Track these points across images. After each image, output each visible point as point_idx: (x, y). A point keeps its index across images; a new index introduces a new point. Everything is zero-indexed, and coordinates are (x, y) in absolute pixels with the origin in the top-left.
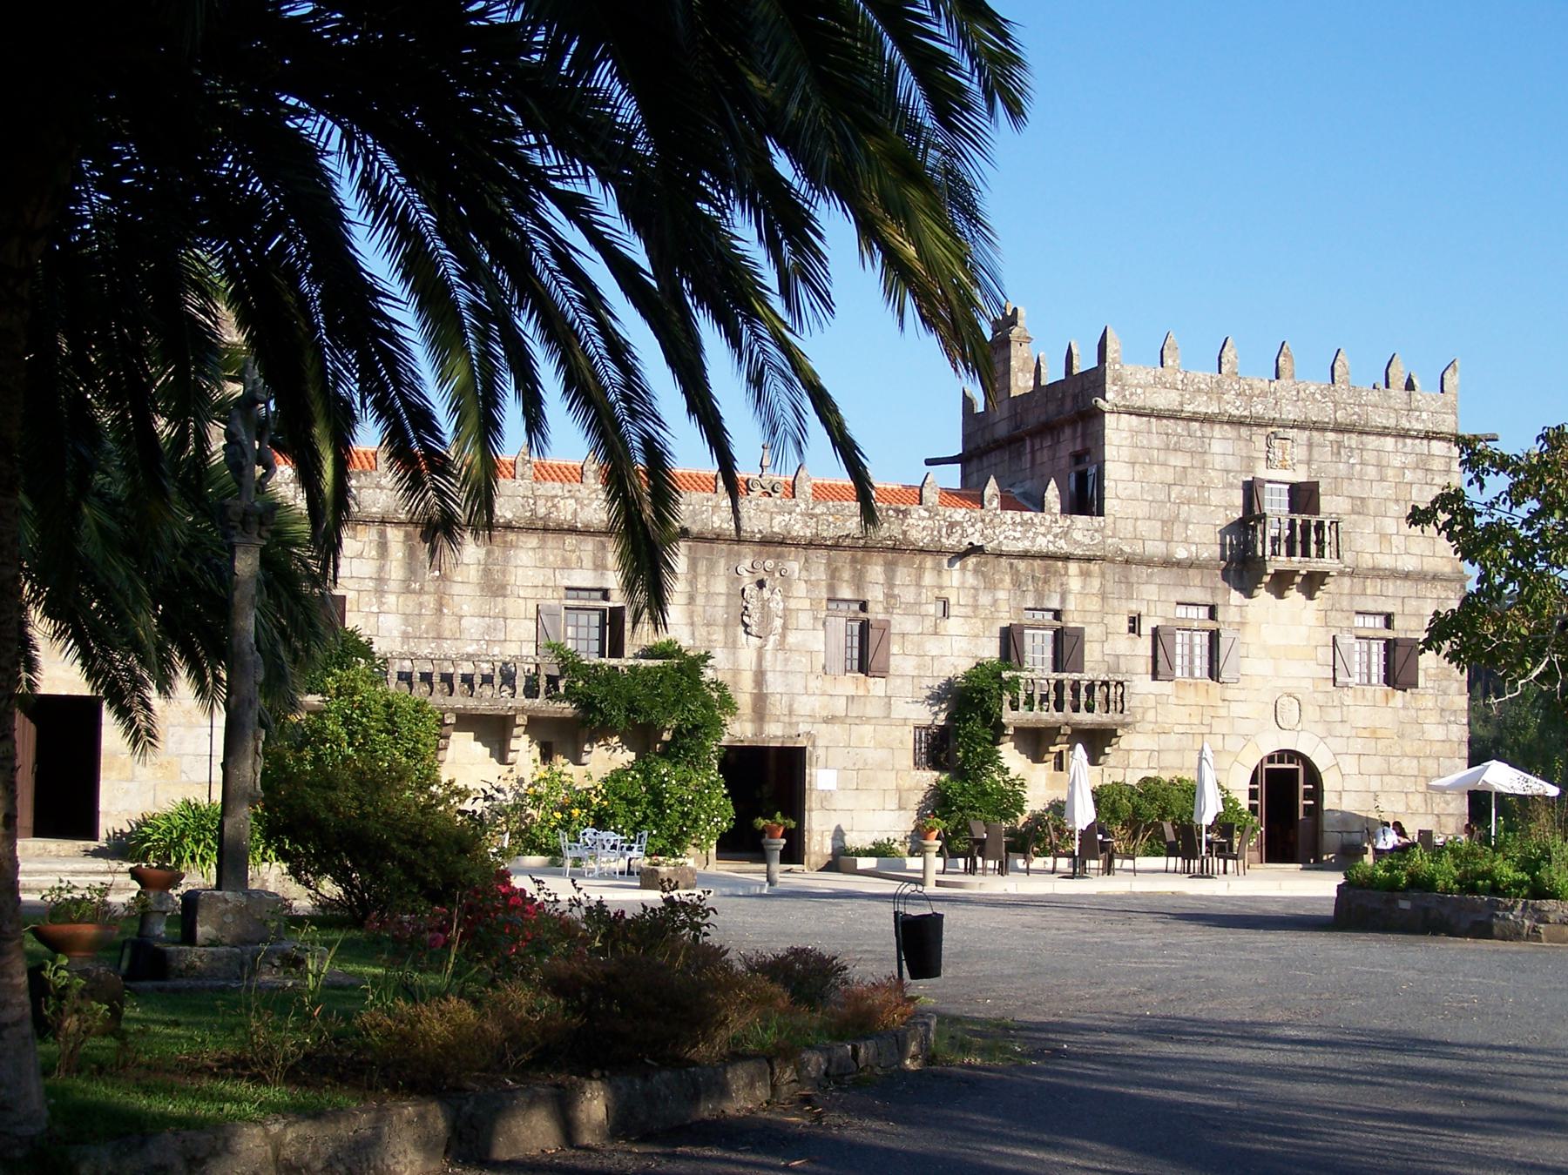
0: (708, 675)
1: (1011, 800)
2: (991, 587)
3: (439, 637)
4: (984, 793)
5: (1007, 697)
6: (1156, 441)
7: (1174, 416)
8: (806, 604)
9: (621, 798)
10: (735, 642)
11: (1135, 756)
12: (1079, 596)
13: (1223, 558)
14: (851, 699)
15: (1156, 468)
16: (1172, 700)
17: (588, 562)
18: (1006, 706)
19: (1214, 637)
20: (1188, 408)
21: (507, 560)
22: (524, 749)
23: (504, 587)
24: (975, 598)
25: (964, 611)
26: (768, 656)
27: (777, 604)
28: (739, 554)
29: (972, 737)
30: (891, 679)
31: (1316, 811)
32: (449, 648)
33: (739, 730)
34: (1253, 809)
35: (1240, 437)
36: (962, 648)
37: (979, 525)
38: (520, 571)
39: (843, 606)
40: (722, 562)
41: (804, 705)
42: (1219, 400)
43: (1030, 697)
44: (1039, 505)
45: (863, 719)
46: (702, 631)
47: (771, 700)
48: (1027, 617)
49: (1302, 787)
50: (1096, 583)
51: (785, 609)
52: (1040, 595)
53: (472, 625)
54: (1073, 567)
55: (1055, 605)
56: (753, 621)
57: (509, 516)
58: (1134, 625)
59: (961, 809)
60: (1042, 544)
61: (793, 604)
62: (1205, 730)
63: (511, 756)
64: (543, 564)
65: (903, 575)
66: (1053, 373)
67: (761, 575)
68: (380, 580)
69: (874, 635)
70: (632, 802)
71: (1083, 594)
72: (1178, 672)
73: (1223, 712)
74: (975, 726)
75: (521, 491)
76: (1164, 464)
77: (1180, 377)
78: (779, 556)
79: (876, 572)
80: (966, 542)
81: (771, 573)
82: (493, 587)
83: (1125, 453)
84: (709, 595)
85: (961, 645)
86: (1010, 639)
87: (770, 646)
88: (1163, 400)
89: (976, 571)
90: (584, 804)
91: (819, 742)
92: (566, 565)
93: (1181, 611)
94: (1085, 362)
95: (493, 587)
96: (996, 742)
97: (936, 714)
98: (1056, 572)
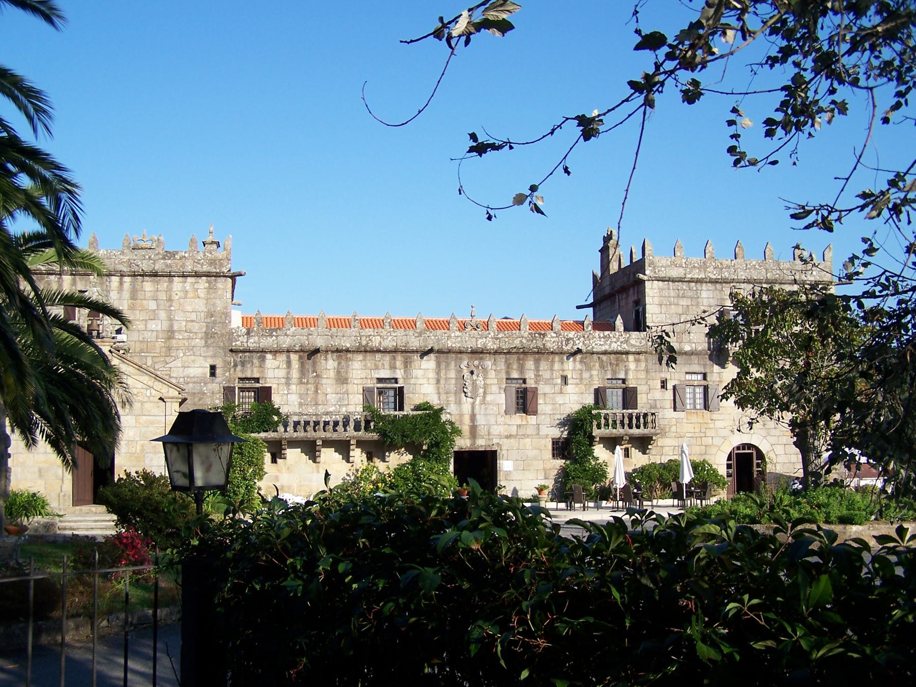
0: (444, 417)
1: (599, 473)
2: (589, 369)
3: (317, 404)
4: (585, 470)
5: (595, 423)
6: (672, 293)
7: (681, 280)
8: (495, 381)
9: (402, 478)
10: (460, 401)
11: (666, 450)
12: (635, 372)
13: (709, 349)
14: (519, 426)
15: (673, 307)
16: (684, 420)
17: (387, 365)
18: (595, 427)
19: (706, 388)
20: (689, 276)
21: (348, 366)
22: (357, 455)
23: (347, 379)
24: (581, 374)
25: (575, 381)
26: (477, 407)
27: (480, 382)
28: (461, 359)
29: (579, 442)
30: (539, 416)
31: (762, 473)
32: (321, 409)
33: (462, 443)
34: (729, 475)
35: (716, 289)
36: (575, 398)
37: (582, 339)
38: (354, 371)
39: (515, 381)
40: (453, 363)
41: (496, 430)
42: (705, 271)
43: (615, 422)
44: (613, 328)
45: (525, 436)
46: (443, 397)
47: (479, 428)
48: (607, 384)
49: (755, 461)
50: (643, 365)
51: (485, 384)
52: (614, 372)
53: (332, 398)
54: (631, 357)
55: (622, 376)
56: (468, 390)
57: (348, 345)
58: (664, 384)
59: (573, 478)
60: (615, 347)
61: (488, 382)
62: (703, 435)
63: (351, 459)
64: (365, 368)
65: (544, 365)
66: (626, 263)
67: (473, 368)
68: (288, 378)
69: (529, 395)
70: (406, 479)
71: (636, 370)
72: (688, 407)
73: (711, 426)
74: (580, 438)
75: (354, 334)
76: (677, 305)
77: (684, 261)
78: (481, 359)
79: (530, 364)
80: (575, 348)
81: (477, 367)
82: (342, 379)
83: (656, 300)
84: (447, 379)
85: (574, 398)
86: (599, 394)
87: (477, 402)
88: (675, 273)
89: (581, 362)
90: (384, 481)
91: (504, 448)
92: (377, 368)
93: (688, 377)
94: (637, 257)
95: (342, 379)
96: (591, 445)
97: (562, 432)
98: (622, 360)
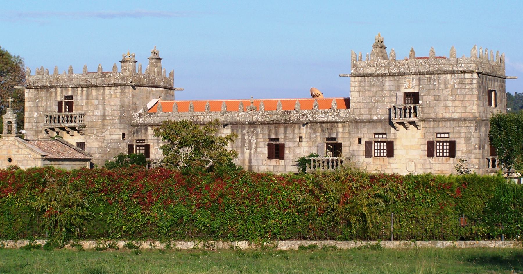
2: (315, 132)
6: (367, 84)
8: (262, 140)
14: (275, 166)
24: (310, 136)
37: (311, 114)
40: (240, 130)
50: (347, 129)
52: (330, 134)
61: (259, 140)
65: (289, 130)
71: (343, 133)
73: (389, 167)
76: (370, 91)
77: (375, 63)
79: (282, 130)
85: (306, 149)
87: (252, 152)
88: (369, 71)
89: (311, 128)
